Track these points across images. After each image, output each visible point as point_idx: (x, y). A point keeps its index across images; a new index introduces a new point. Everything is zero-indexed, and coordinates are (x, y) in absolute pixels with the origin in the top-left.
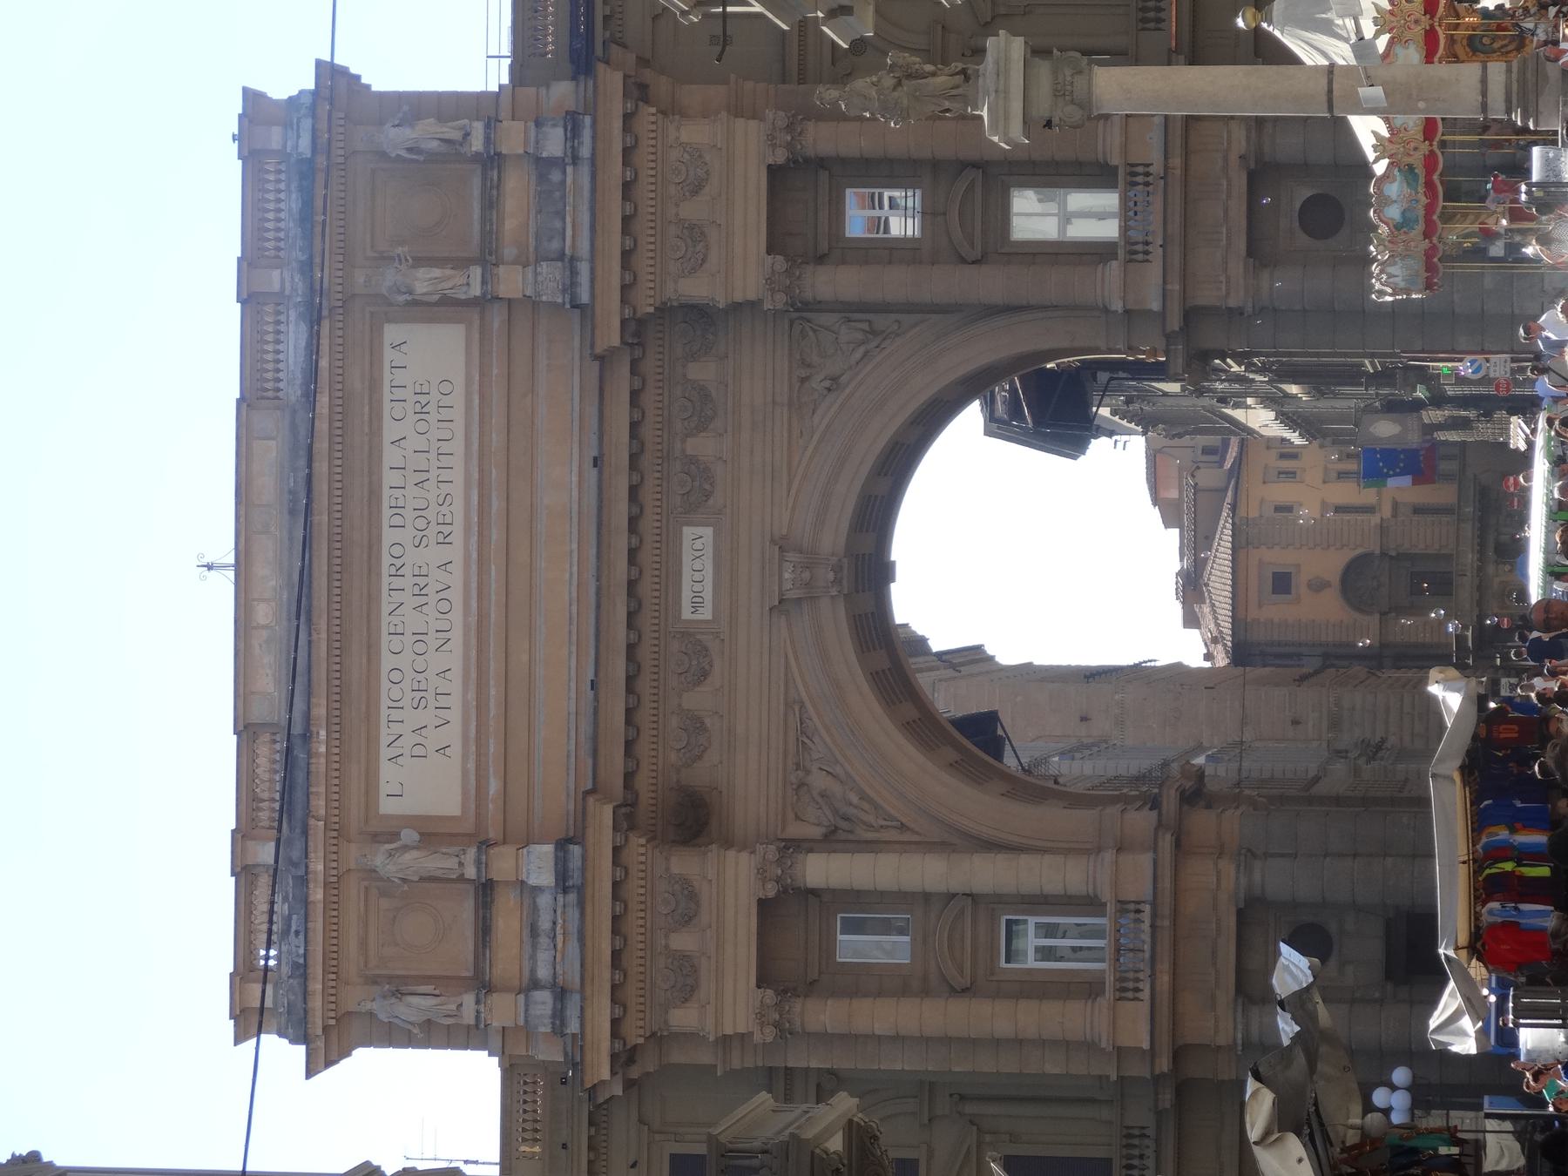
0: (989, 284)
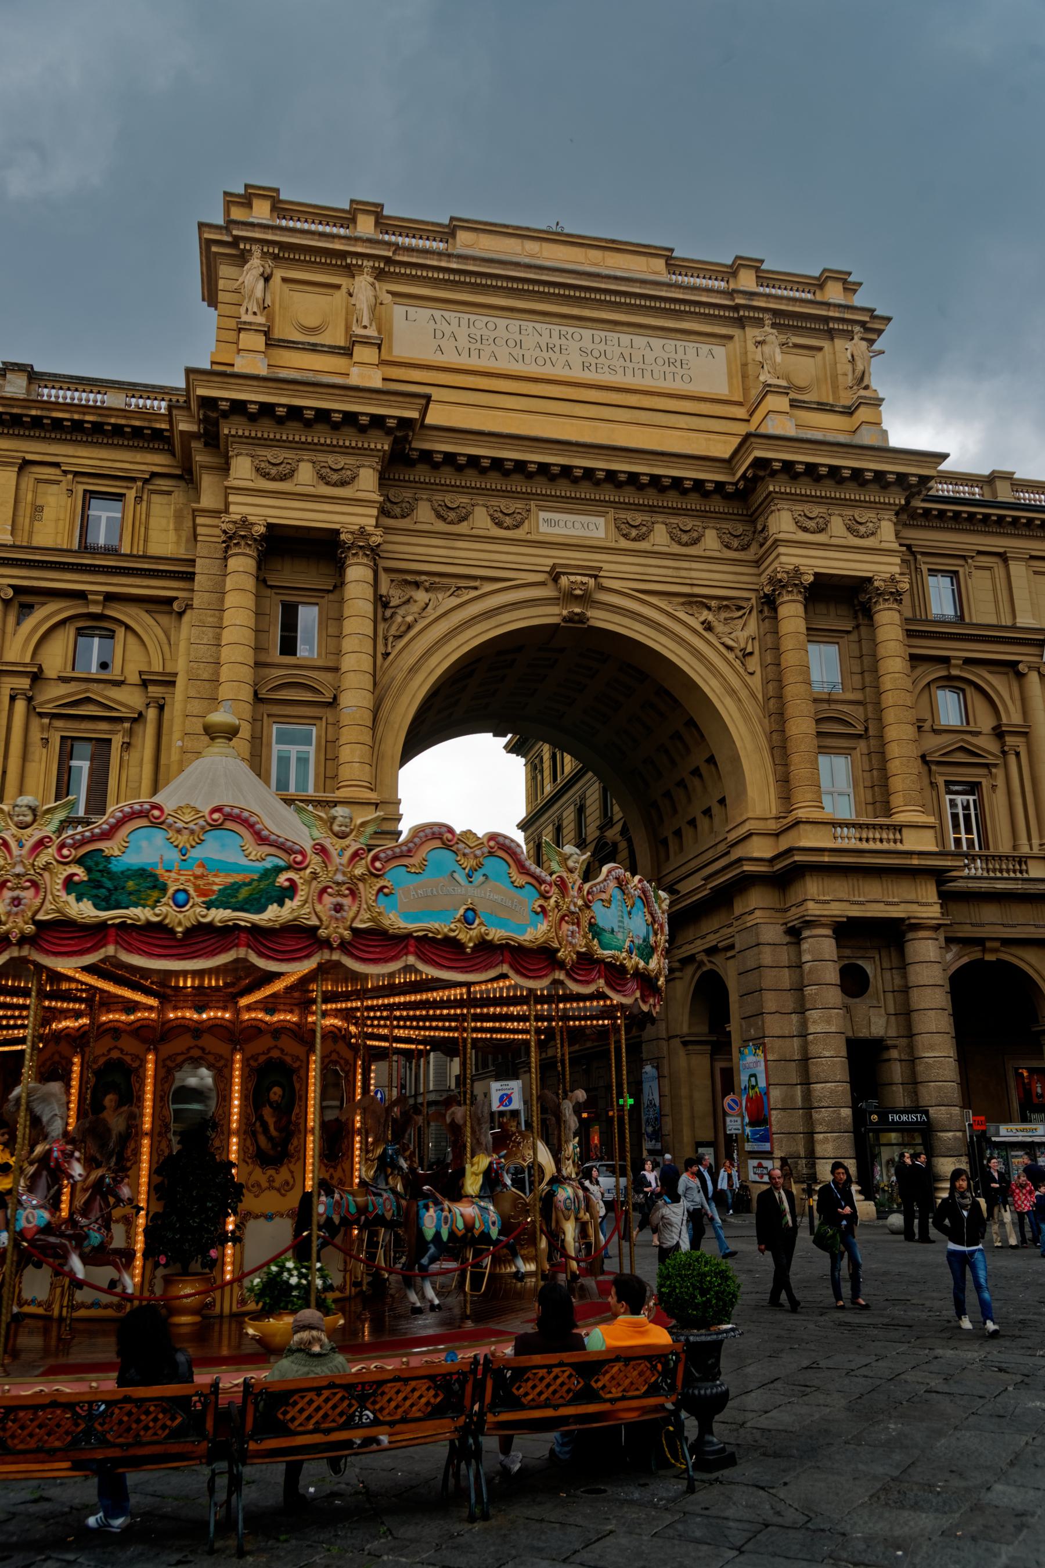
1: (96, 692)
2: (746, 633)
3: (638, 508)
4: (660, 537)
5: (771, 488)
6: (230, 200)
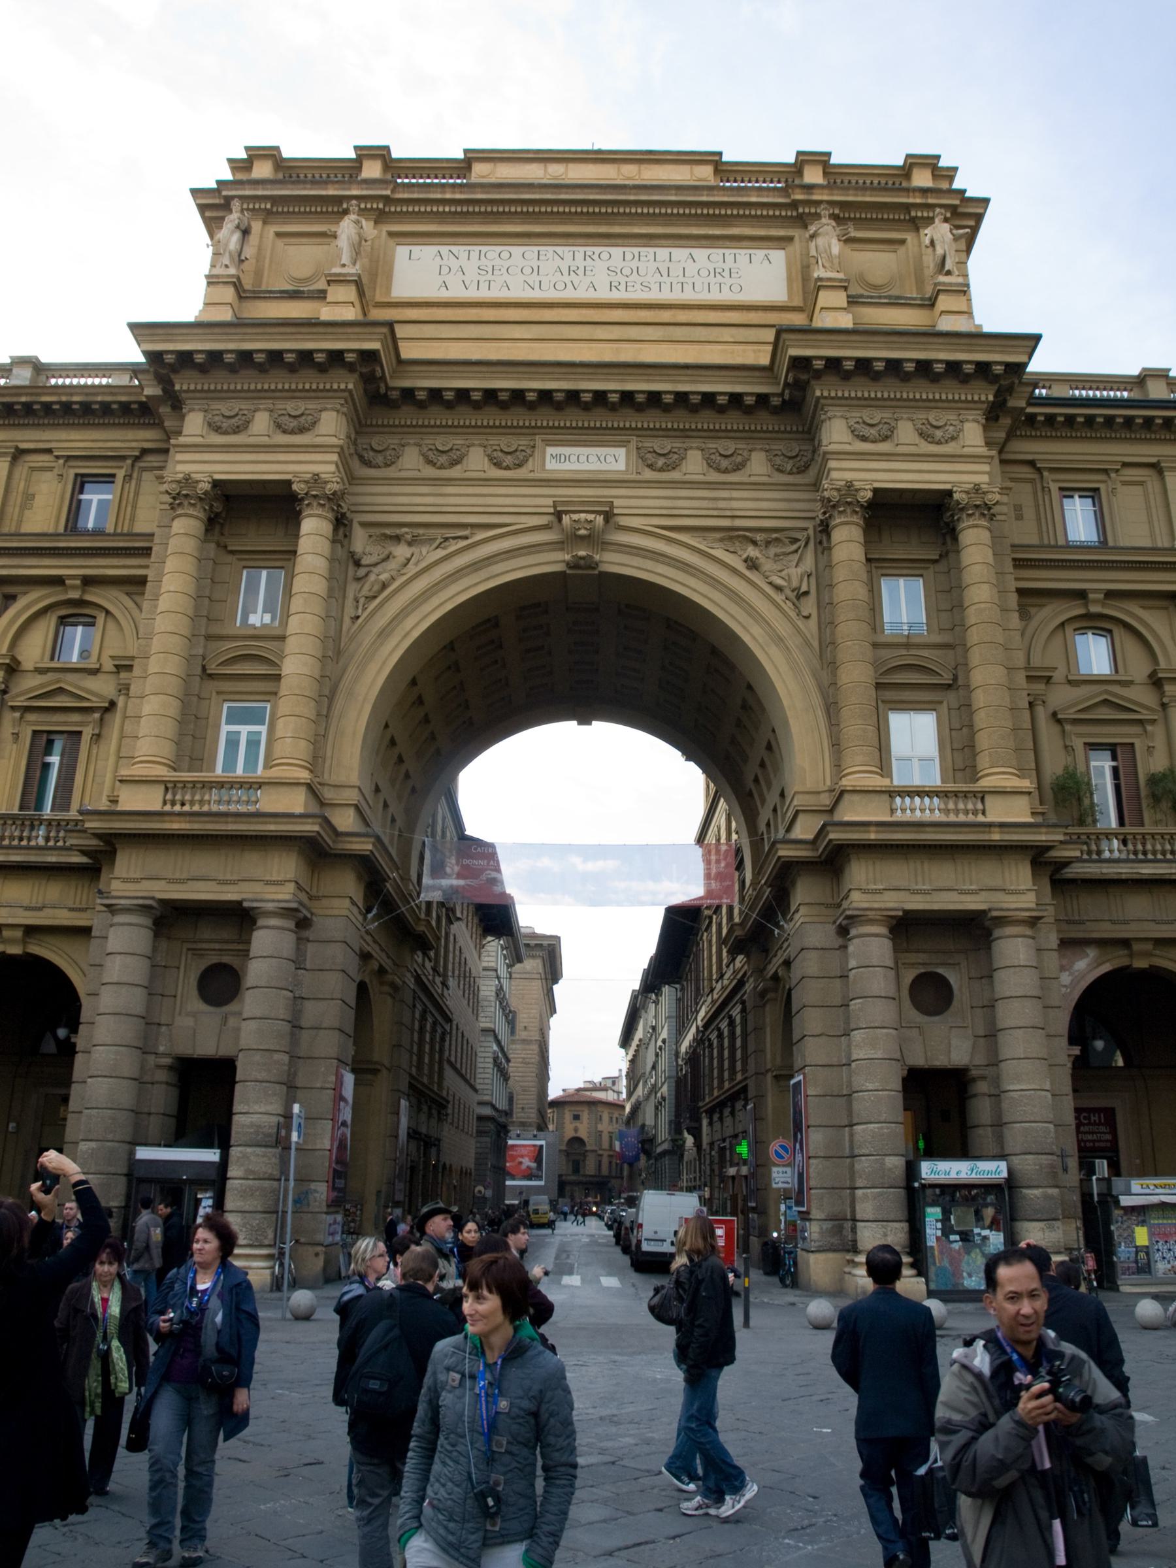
1: (70, 682)
2: (799, 570)
3: (667, 433)
4: (694, 464)
5: (818, 393)
6: (234, 164)
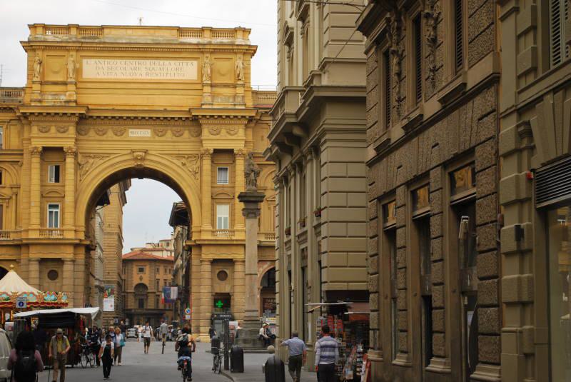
0: (207, 200)
2: (197, 166)
4: (169, 135)
